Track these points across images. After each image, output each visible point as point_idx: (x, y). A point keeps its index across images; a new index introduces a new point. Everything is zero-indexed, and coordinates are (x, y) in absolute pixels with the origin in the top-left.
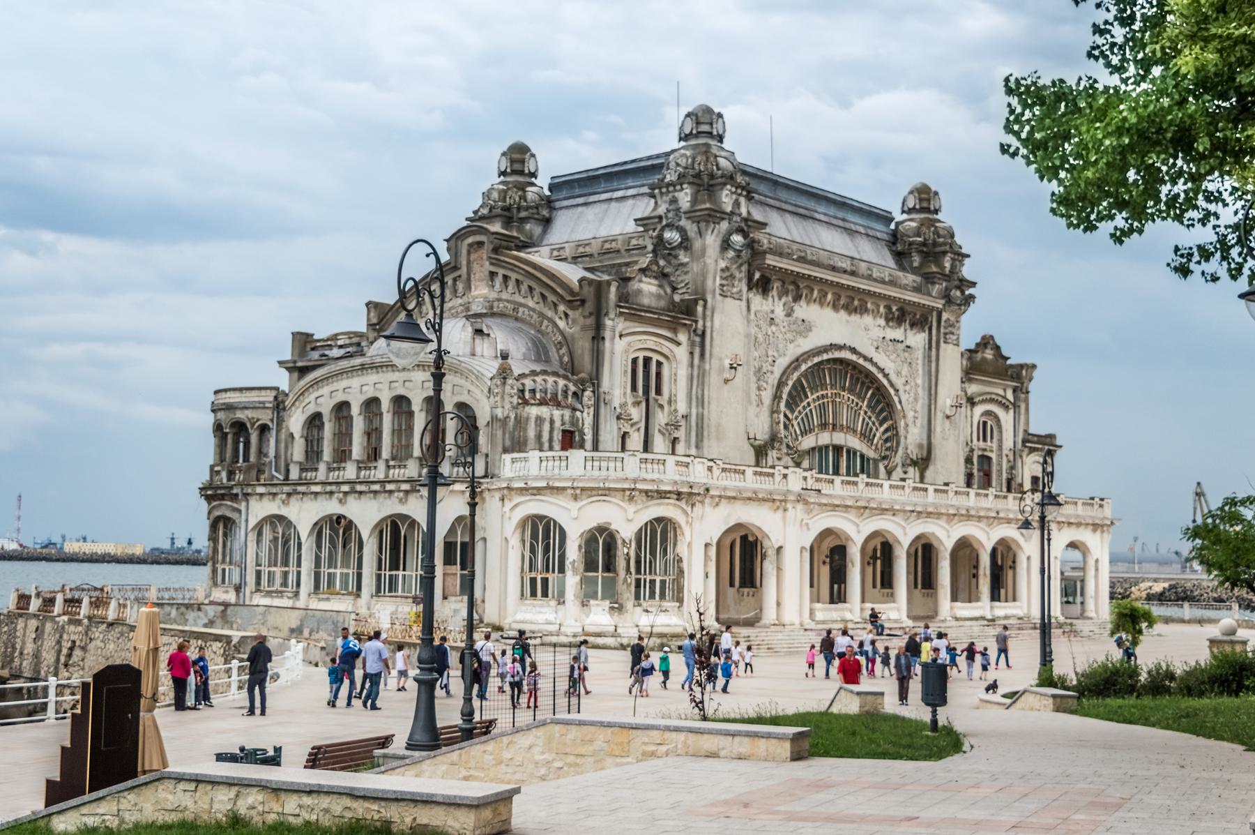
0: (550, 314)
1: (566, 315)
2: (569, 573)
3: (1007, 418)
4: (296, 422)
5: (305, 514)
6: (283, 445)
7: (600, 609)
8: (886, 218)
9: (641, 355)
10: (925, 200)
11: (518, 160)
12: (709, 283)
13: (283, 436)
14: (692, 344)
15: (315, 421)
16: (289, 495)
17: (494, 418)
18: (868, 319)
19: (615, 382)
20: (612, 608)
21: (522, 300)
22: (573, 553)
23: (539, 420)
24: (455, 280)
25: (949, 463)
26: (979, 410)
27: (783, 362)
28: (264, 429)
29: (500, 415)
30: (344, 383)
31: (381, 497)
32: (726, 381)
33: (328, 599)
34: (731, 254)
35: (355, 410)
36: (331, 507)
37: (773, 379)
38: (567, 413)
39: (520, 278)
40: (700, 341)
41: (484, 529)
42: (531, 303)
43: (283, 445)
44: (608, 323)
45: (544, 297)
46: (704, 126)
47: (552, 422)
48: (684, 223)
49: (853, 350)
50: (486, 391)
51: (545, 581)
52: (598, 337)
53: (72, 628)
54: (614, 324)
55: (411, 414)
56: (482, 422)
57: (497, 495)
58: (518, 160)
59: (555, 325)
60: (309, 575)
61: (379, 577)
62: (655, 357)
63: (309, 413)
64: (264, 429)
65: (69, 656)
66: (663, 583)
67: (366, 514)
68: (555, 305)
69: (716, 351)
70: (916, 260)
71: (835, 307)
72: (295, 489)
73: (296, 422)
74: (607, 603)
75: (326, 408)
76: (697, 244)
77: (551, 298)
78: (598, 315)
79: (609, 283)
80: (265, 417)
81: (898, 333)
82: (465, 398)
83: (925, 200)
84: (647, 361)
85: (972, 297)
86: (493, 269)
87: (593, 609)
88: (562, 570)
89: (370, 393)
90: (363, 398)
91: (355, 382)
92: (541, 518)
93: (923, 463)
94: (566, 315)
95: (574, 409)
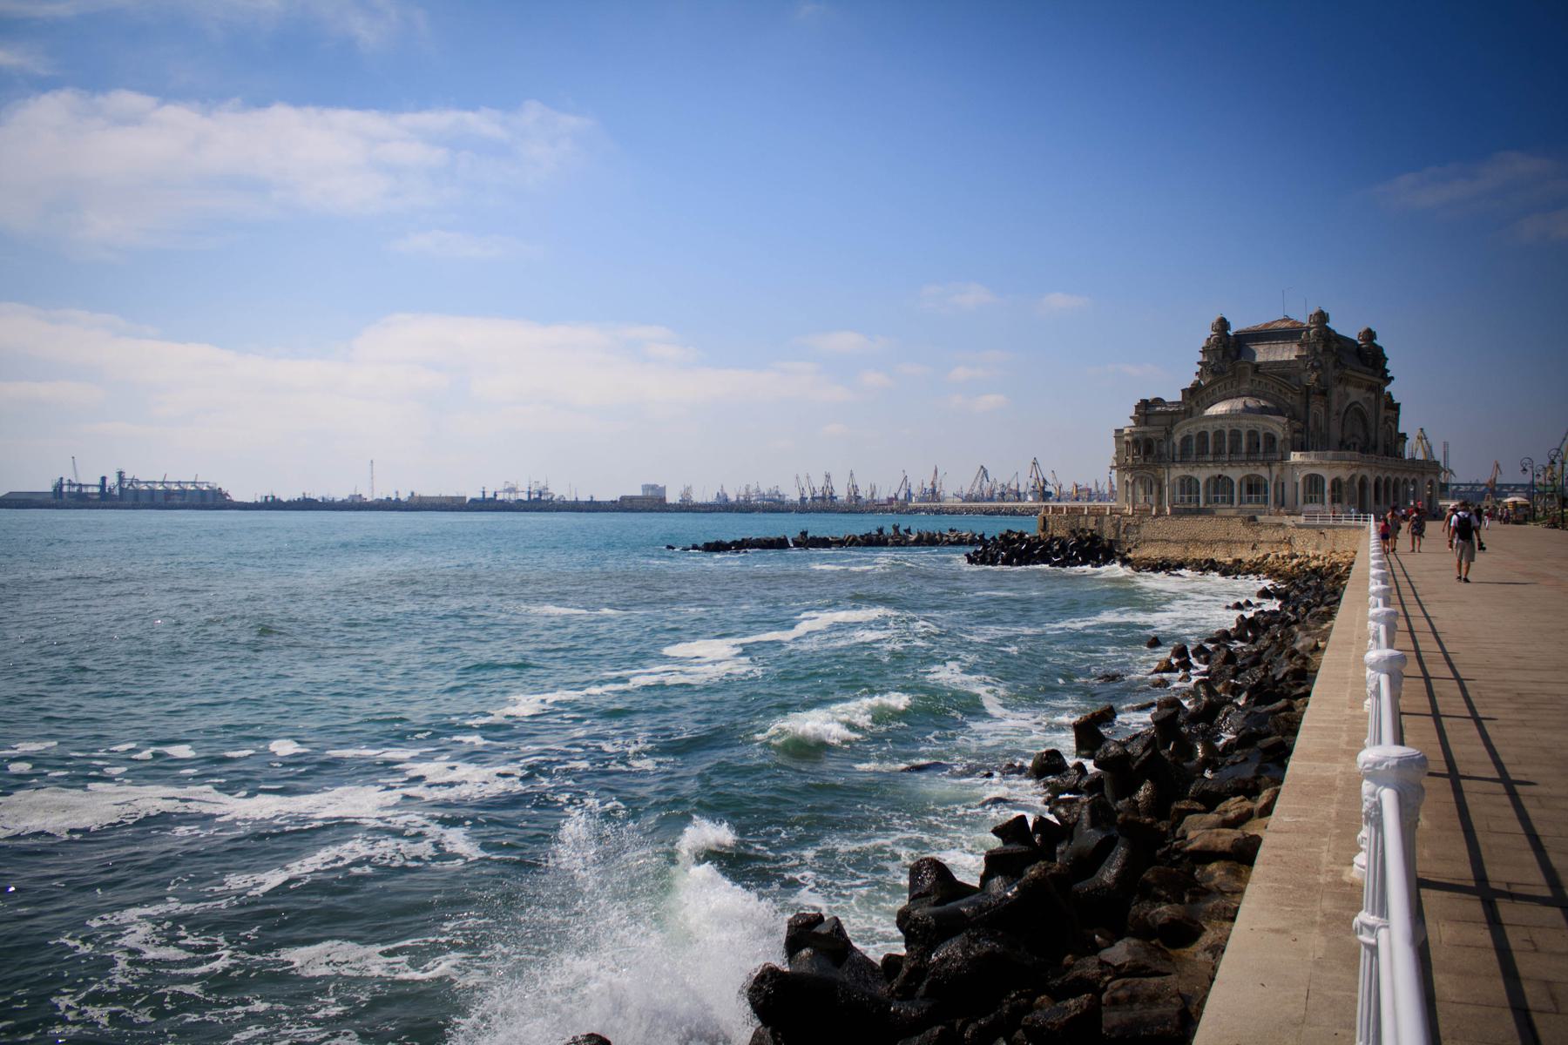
4: (1177, 438)
5: (1202, 475)
8: (1354, 342)
10: (1370, 335)
11: (1223, 324)
15: (1186, 440)
19: (1311, 422)
22: (1327, 486)
25: (1381, 448)
36: (1217, 472)
58: (1223, 324)
67: (1236, 474)
72: (1199, 463)
73: (1177, 438)
75: (1194, 433)
78: (1308, 397)
80: (1161, 435)
83: (1370, 335)
91: (1210, 424)
93: (1375, 447)
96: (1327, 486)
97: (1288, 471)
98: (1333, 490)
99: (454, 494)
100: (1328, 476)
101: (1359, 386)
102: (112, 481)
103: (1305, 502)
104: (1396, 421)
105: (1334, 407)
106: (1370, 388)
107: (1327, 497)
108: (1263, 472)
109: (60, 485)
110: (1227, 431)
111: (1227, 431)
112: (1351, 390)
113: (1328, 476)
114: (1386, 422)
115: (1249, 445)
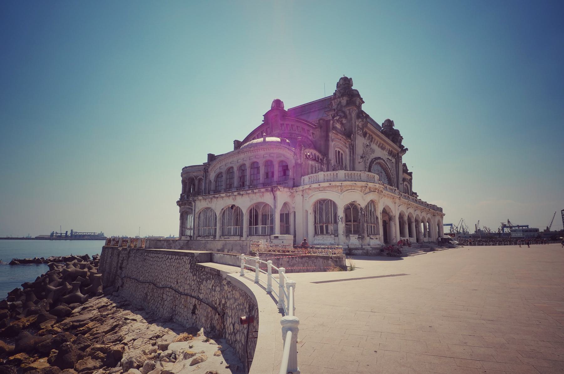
0: (305, 135)
1: (313, 133)
2: (340, 223)
3: (409, 187)
4: (212, 176)
6: (207, 185)
7: (354, 238)
9: (338, 149)
10: (389, 123)
11: (278, 104)
12: (354, 129)
13: (207, 182)
14: (350, 149)
15: (219, 176)
16: (211, 199)
17: (297, 164)
18: (385, 152)
20: (359, 238)
21: (293, 132)
23: (312, 165)
24: (267, 129)
26: (405, 183)
27: (370, 160)
28: (200, 180)
29: (299, 162)
30: (231, 160)
31: (251, 195)
32: (359, 162)
33: (229, 238)
34: (360, 120)
35: (235, 169)
37: (368, 164)
38: (319, 165)
39: (293, 123)
40: (352, 148)
41: (294, 208)
42: (297, 133)
43: (207, 185)
44: (330, 135)
45: (303, 129)
46: (351, 79)
47: (315, 168)
48: (343, 109)
49: (384, 161)
50: (292, 153)
51: (327, 227)
52: (327, 138)
53: (123, 252)
54: (332, 135)
55: (258, 168)
56: (290, 167)
57: (301, 193)
59: (308, 138)
60: (220, 229)
61: (250, 229)
62: (341, 152)
63: (217, 173)
64: (200, 180)
65: (122, 263)
66: (374, 226)
68: (308, 131)
69: (357, 152)
70: (391, 137)
71: (379, 146)
73: (212, 176)
74: (357, 236)
75: (224, 170)
76: (349, 117)
77: (306, 128)
78: (327, 132)
79: (330, 120)
81: (390, 158)
82: (282, 158)
83: (389, 123)
84: (339, 152)
85: (407, 149)
86: (282, 122)
87: (351, 238)
88: (336, 222)
89: (241, 162)
90: (238, 164)
91: (235, 159)
92: (324, 200)
94: (313, 133)
95: (322, 164)
96: (341, 213)
97: (298, 198)
98: (348, 220)
99: (158, 236)
100: (342, 201)
101: (383, 148)
102: (69, 234)
103: (316, 233)
104: (410, 181)
105: (359, 150)
106: (394, 156)
107: (341, 226)
108: (267, 198)
109: (53, 233)
110: (248, 164)
111: (248, 164)
112: (374, 146)
113: (342, 201)
114: (404, 180)
115: (267, 174)
